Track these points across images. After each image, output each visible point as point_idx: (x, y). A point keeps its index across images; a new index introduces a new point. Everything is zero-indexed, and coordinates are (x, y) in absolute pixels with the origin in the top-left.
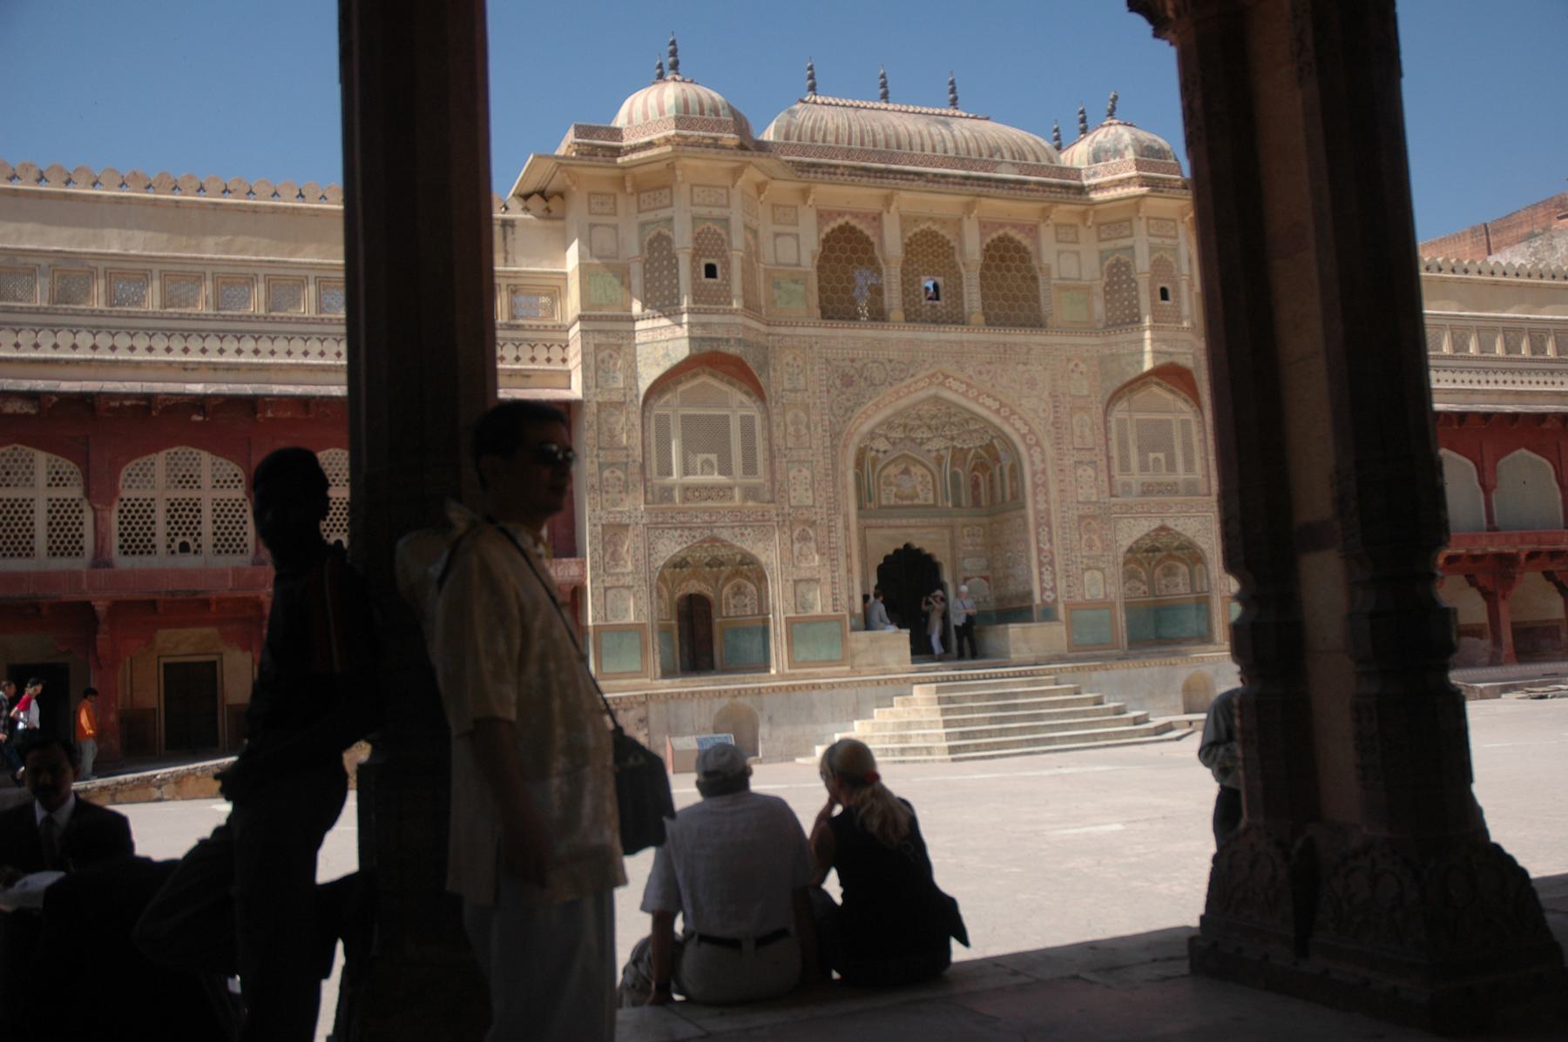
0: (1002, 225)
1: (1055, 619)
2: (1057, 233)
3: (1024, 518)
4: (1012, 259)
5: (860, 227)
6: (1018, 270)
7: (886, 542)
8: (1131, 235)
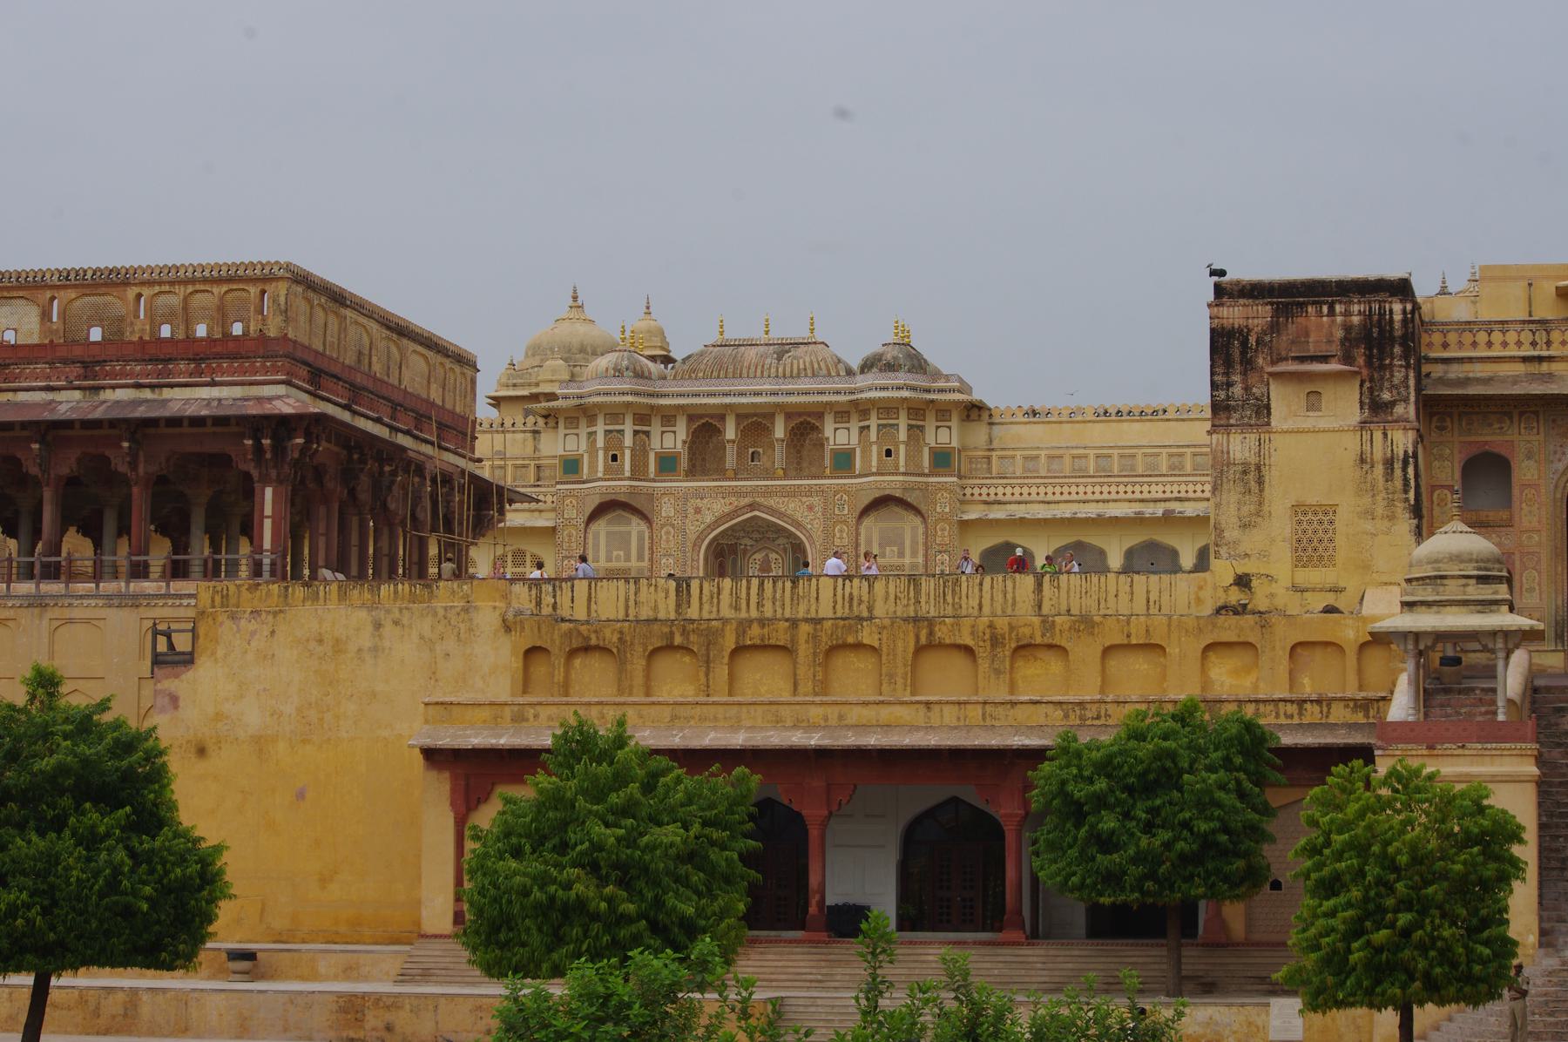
0: (800, 414)
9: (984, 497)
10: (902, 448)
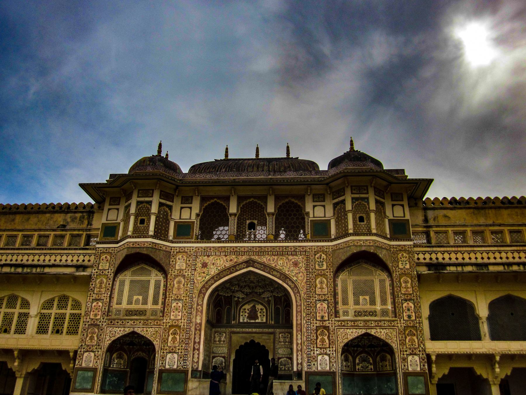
0: (287, 197)
2: (313, 198)
6: (295, 215)
8: (344, 195)
9: (428, 261)
10: (373, 216)
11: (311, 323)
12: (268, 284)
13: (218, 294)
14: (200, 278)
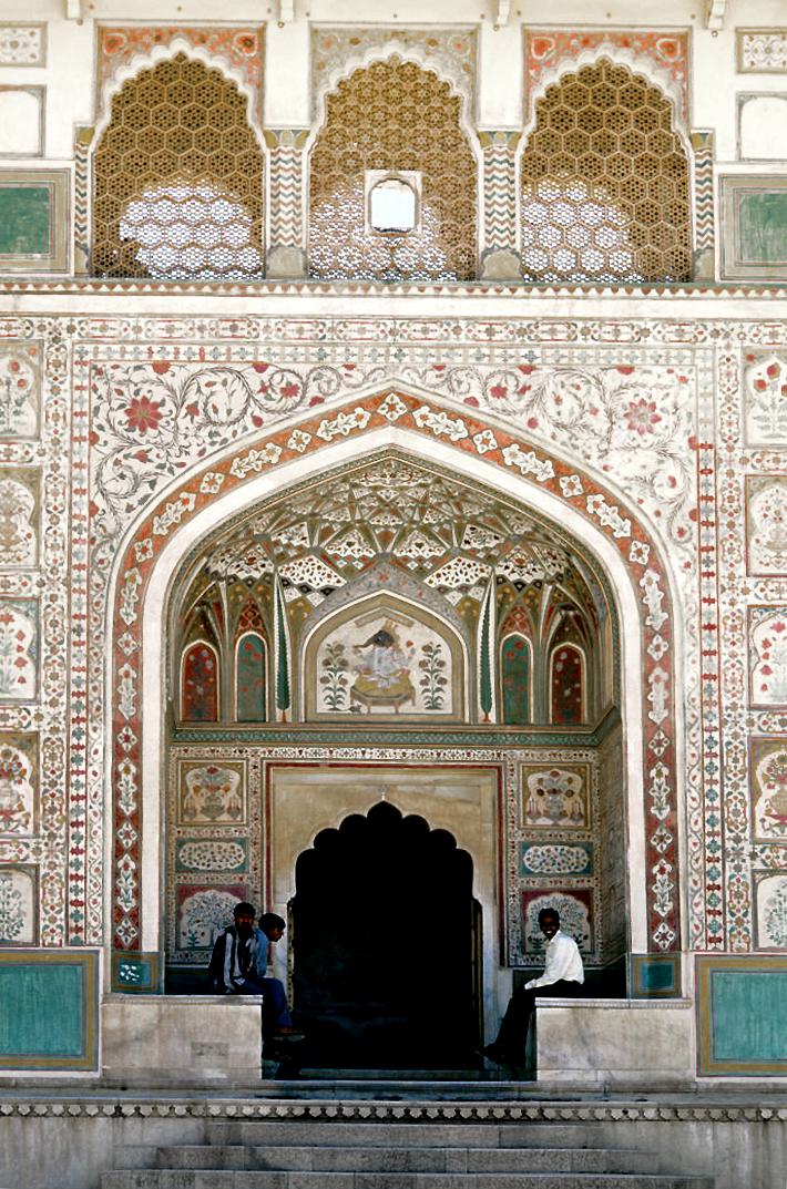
1: (677, 994)
3: (620, 743)
4: (615, 119)
5: (212, 63)
6: (632, 145)
7: (316, 798)
11: (723, 723)
12: (473, 520)
13: (206, 570)
14: (125, 486)
